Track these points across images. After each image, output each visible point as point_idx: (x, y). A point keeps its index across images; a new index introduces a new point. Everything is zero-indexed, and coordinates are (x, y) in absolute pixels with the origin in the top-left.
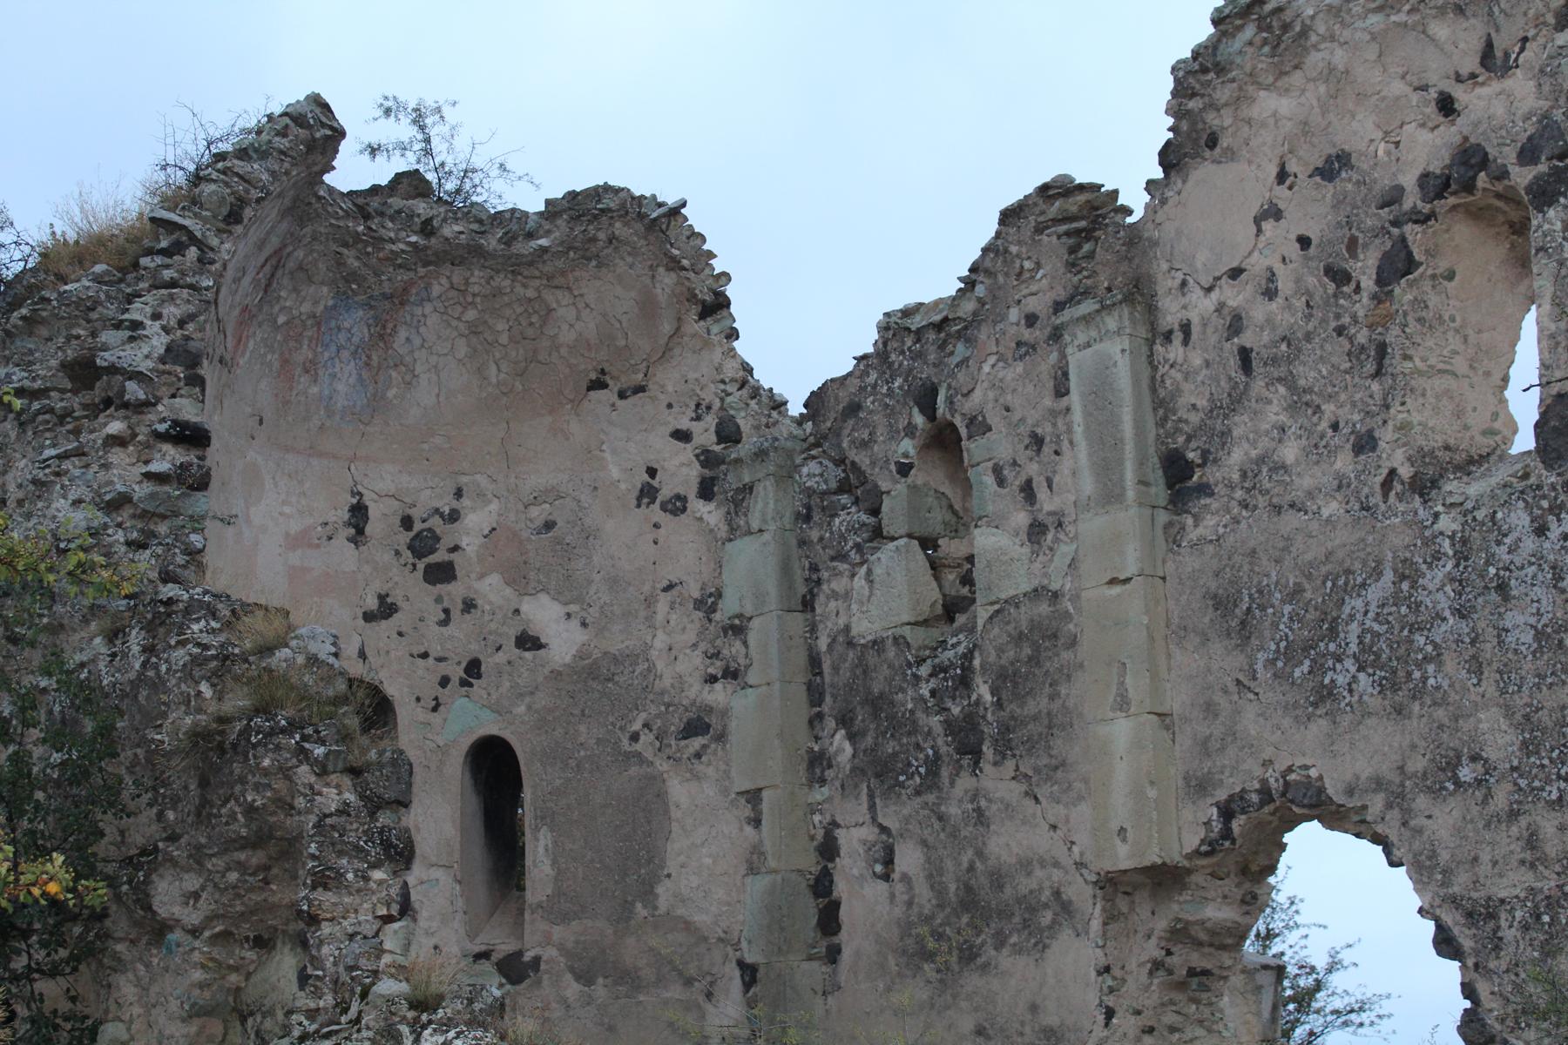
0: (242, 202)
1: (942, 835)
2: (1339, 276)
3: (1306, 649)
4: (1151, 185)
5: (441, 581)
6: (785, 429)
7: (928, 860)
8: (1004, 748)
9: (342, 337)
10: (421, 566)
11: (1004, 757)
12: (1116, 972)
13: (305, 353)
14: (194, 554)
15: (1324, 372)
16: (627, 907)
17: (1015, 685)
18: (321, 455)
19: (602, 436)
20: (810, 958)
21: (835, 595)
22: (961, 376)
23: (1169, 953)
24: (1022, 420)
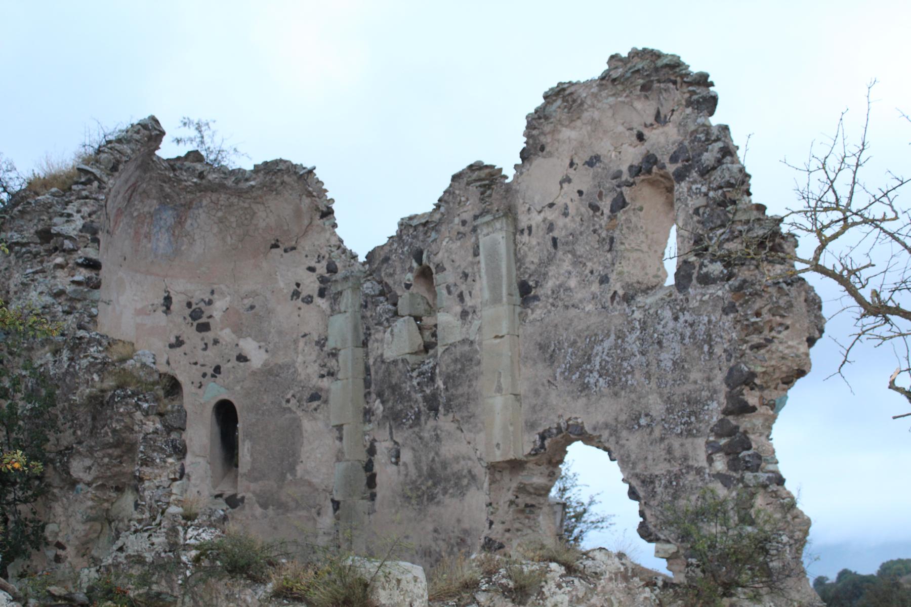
0: (118, 162)
1: (421, 446)
2: (595, 208)
3: (577, 368)
4: (516, 167)
6: (357, 267)
7: (415, 457)
8: (448, 408)
9: (162, 223)
10: (195, 324)
11: (448, 411)
12: (494, 505)
13: (145, 229)
14: (93, 317)
15: (588, 249)
17: (454, 380)
19: (277, 269)
20: (363, 498)
21: (377, 340)
22: (434, 246)
23: (517, 497)
24: (459, 266)
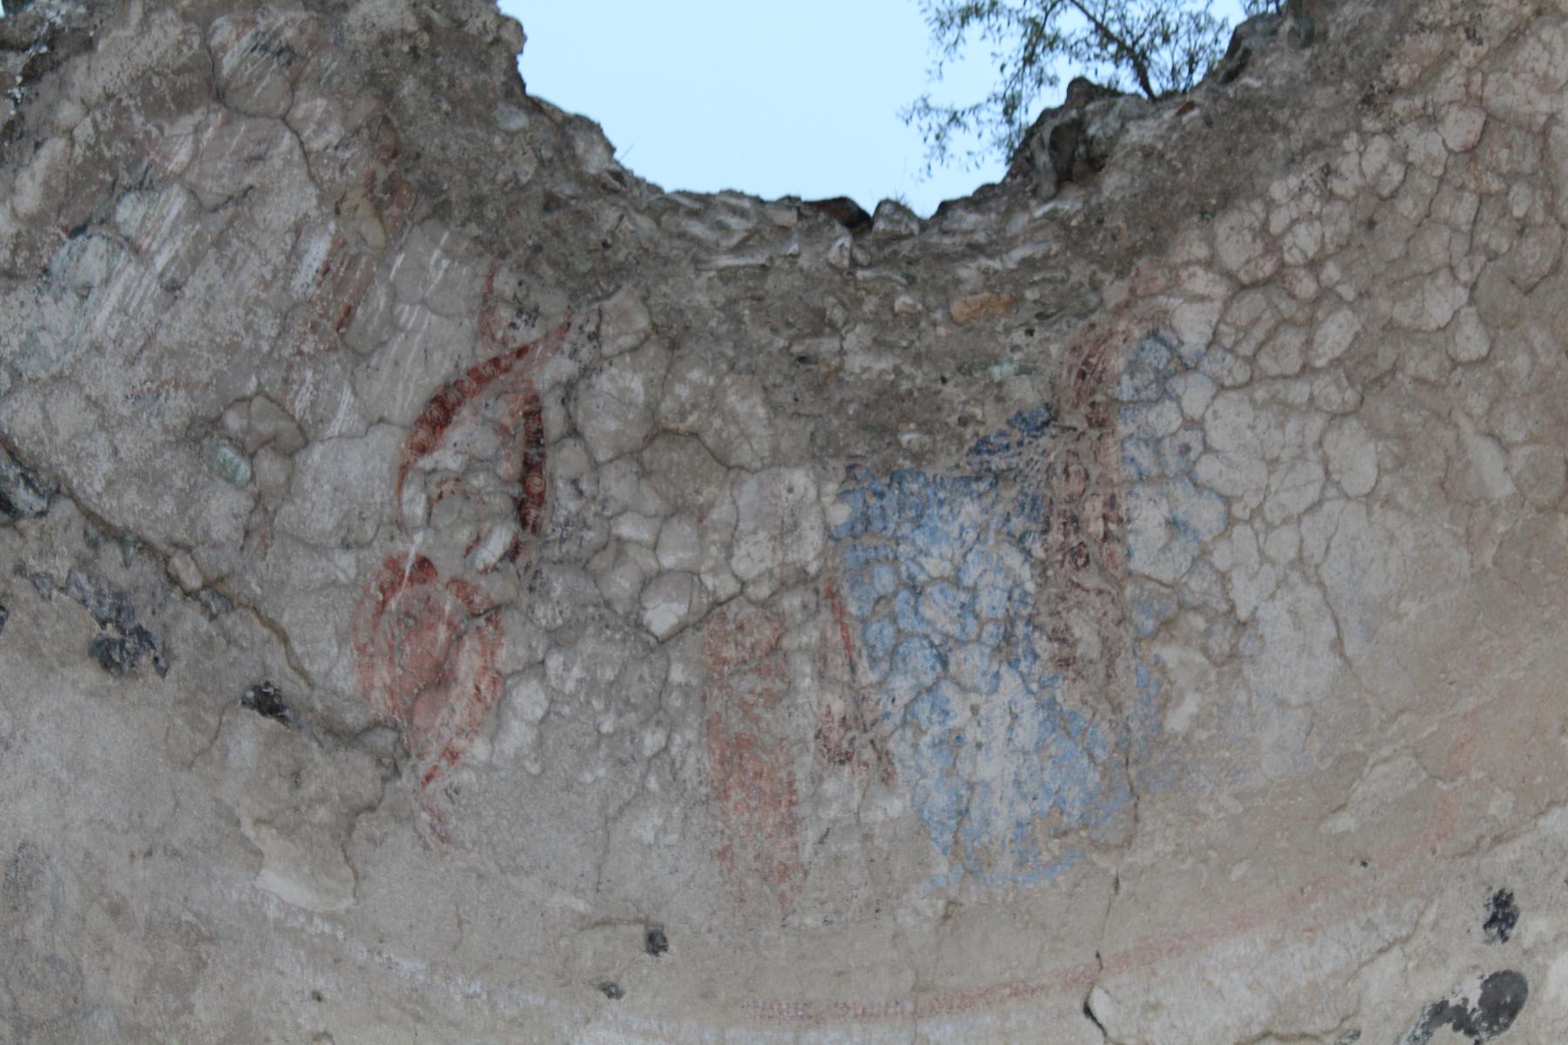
9: (938, 611)
18: (961, 1002)
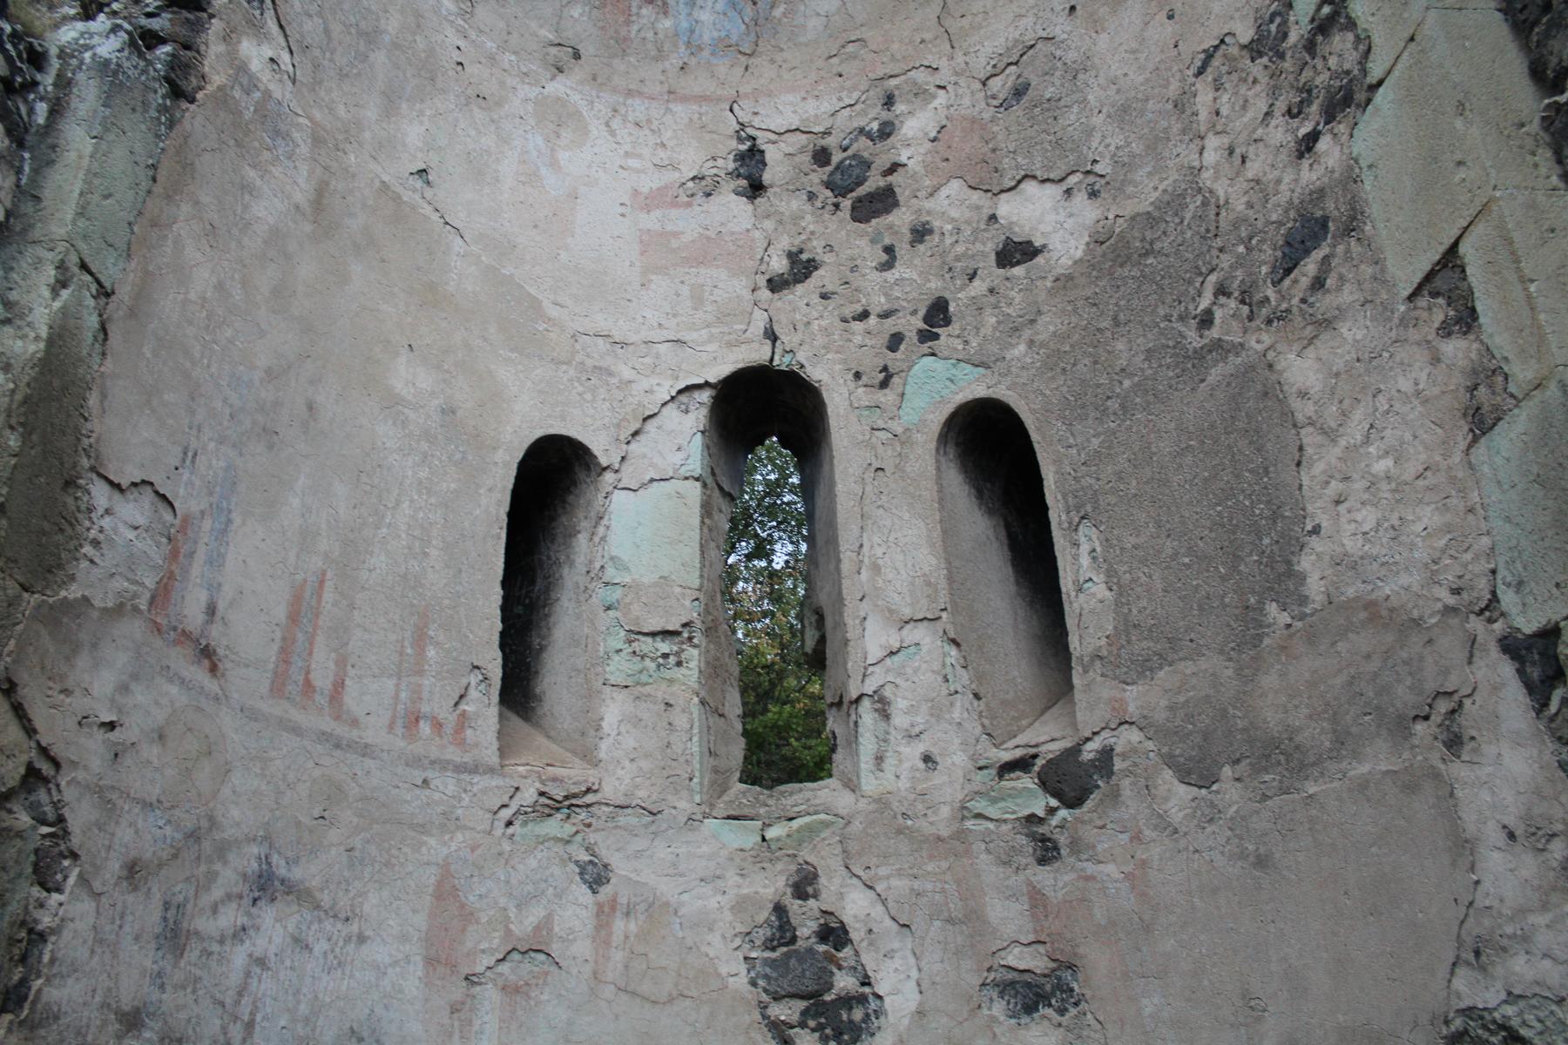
5: (877, 214)
10: (846, 203)
16: (1252, 618)
18: (685, 99)
